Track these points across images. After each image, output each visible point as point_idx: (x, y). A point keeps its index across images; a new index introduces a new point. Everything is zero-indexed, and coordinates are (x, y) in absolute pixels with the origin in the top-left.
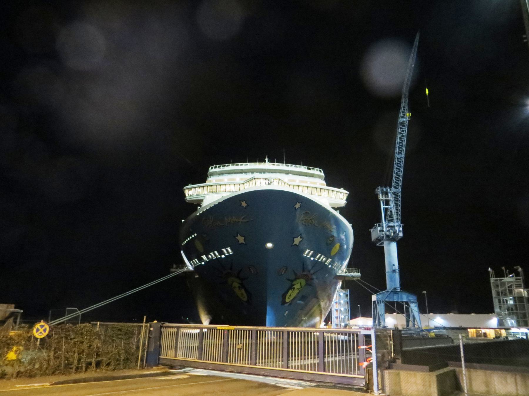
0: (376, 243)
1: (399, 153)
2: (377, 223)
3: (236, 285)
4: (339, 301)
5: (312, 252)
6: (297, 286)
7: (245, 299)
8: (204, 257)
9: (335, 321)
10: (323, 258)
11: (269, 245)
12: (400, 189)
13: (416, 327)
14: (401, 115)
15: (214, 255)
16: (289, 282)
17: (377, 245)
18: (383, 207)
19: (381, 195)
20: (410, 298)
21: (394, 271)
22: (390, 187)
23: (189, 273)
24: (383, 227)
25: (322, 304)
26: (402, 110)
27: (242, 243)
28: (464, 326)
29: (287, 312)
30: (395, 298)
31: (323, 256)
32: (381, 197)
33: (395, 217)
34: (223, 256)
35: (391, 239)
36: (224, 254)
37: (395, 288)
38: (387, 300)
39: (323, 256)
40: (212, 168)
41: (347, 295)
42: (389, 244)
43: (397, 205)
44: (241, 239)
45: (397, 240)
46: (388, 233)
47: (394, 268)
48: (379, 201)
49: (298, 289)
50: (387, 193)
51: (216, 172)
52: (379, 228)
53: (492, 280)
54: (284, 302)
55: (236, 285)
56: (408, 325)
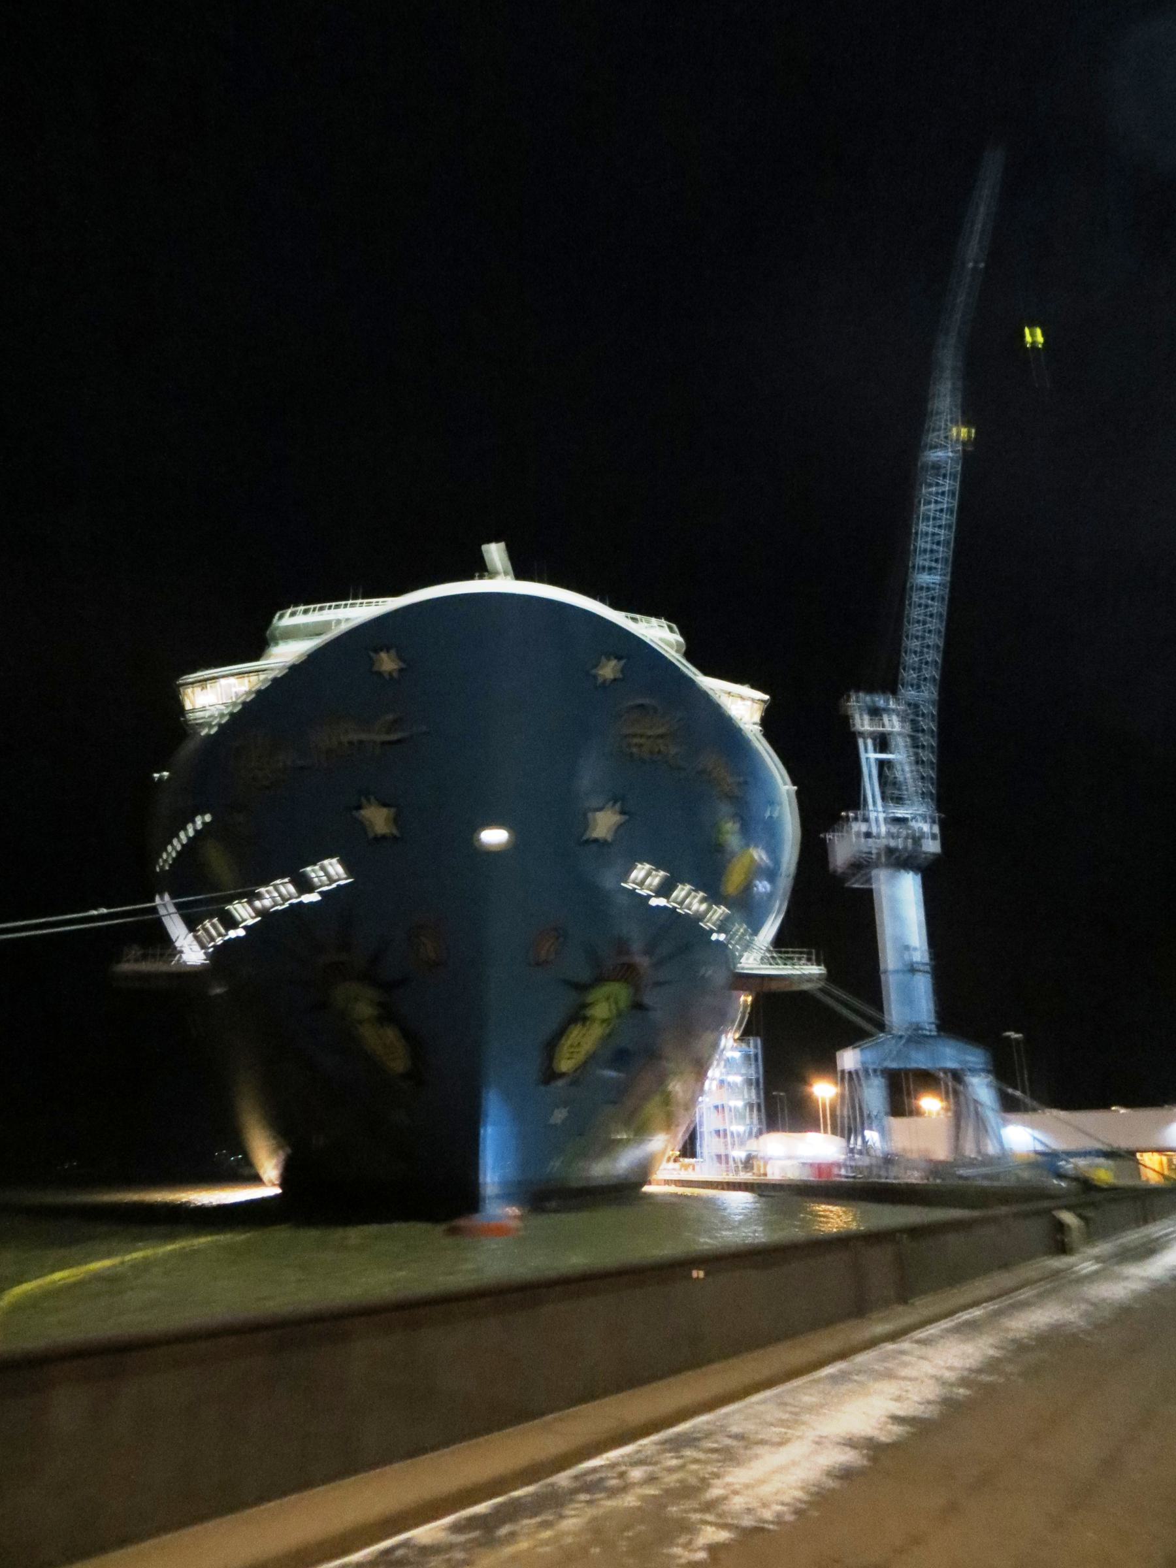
3: (364, 1009)
4: (728, 1072)
9: (708, 1145)
11: (494, 837)
15: (278, 894)
18: (869, 756)
20: (970, 1058)
21: (912, 969)
25: (677, 1087)
28: (1124, 1143)
30: (919, 1060)
32: (863, 724)
34: (308, 898)
35: (900, 860)
38: (894, 1065)
43: (916, 745)
44: (378, 819)
54: (550, 1075)
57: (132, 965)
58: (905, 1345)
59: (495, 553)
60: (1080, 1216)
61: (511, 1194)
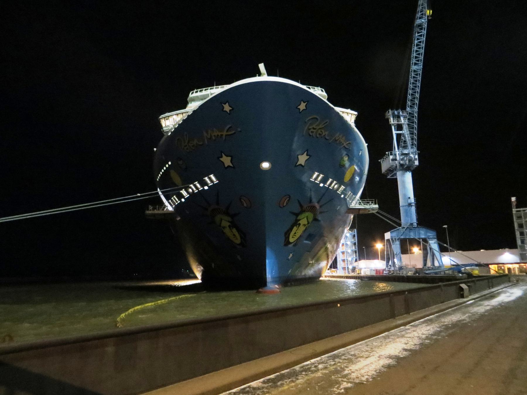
0: (388, 174)
1: (415, 64)
2: (388, 151)
3: (225, 223)
5: (321, 175)
6: (303, 221)
7: (238, 241)
8: (184, 192)
9: (340, 264)
10: (335, 185)
11: (266, 165)
12: (416, 109)
13: (436, 264)
14: (419, 15)
15: (195, 187)
16: (293, 218)
17: (388, 177)
18: (394, 132)
19: (392, 119)
21: (410, 205)
22: (404, 108)
23: (170, 214)
24: (395, 155)
25: (329, 246)
26: (419, 9)
27: (229, 166)
29: (291, 255)
30: (412, 235)
31: (335, 182)
32: (392, 121)
33: (409, 143)
34: (206, 188)
35: (405, 168)
36: (207, 184)
37: (412, 224)
38: (402, 237)
39: (335, 182)
40: (192, 93)
41: (354, 236)
42: (403, 175)
43: (410, 127)
44: (227, 161)
45: (412, 169)
46: (402, 162)
47: (409, 201)
48: (390, 126)
49: (304, 225)
50: (398, 117)
51: (197, 97)
52: (391, 157)
53: (514, 210)
54: (287, 243)
55: (225, 223)
56: (425, 264)
57: (150, 211)
58: (408, 327)
59: (262, 66)
60: (468, 286)
61: (275, 282)
